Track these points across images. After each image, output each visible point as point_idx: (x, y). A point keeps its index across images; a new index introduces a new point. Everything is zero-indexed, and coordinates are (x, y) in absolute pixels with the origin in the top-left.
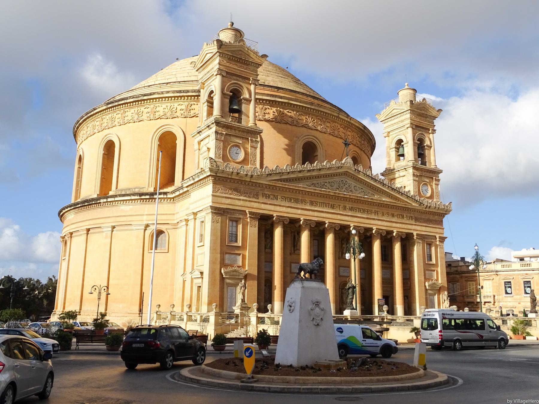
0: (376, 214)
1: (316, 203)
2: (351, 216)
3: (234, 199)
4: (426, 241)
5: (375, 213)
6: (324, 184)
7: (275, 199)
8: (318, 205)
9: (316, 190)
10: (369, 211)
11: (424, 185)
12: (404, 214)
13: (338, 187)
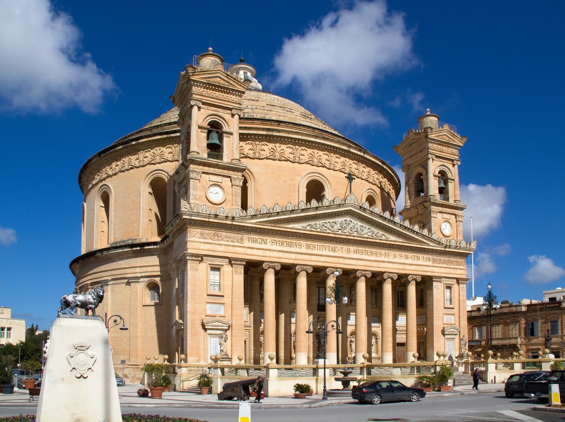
0: (387, 256)
1: (314, 246)
3: (214, 244)
4: (446, 284)
5: (385, 255)
6: (323, 225)
7: (264, 243)
8: (316, 249)
9: (312, 231)
10: (377, 253)
11: (445, 223)
12: (420, 255)
13: (340, 228)
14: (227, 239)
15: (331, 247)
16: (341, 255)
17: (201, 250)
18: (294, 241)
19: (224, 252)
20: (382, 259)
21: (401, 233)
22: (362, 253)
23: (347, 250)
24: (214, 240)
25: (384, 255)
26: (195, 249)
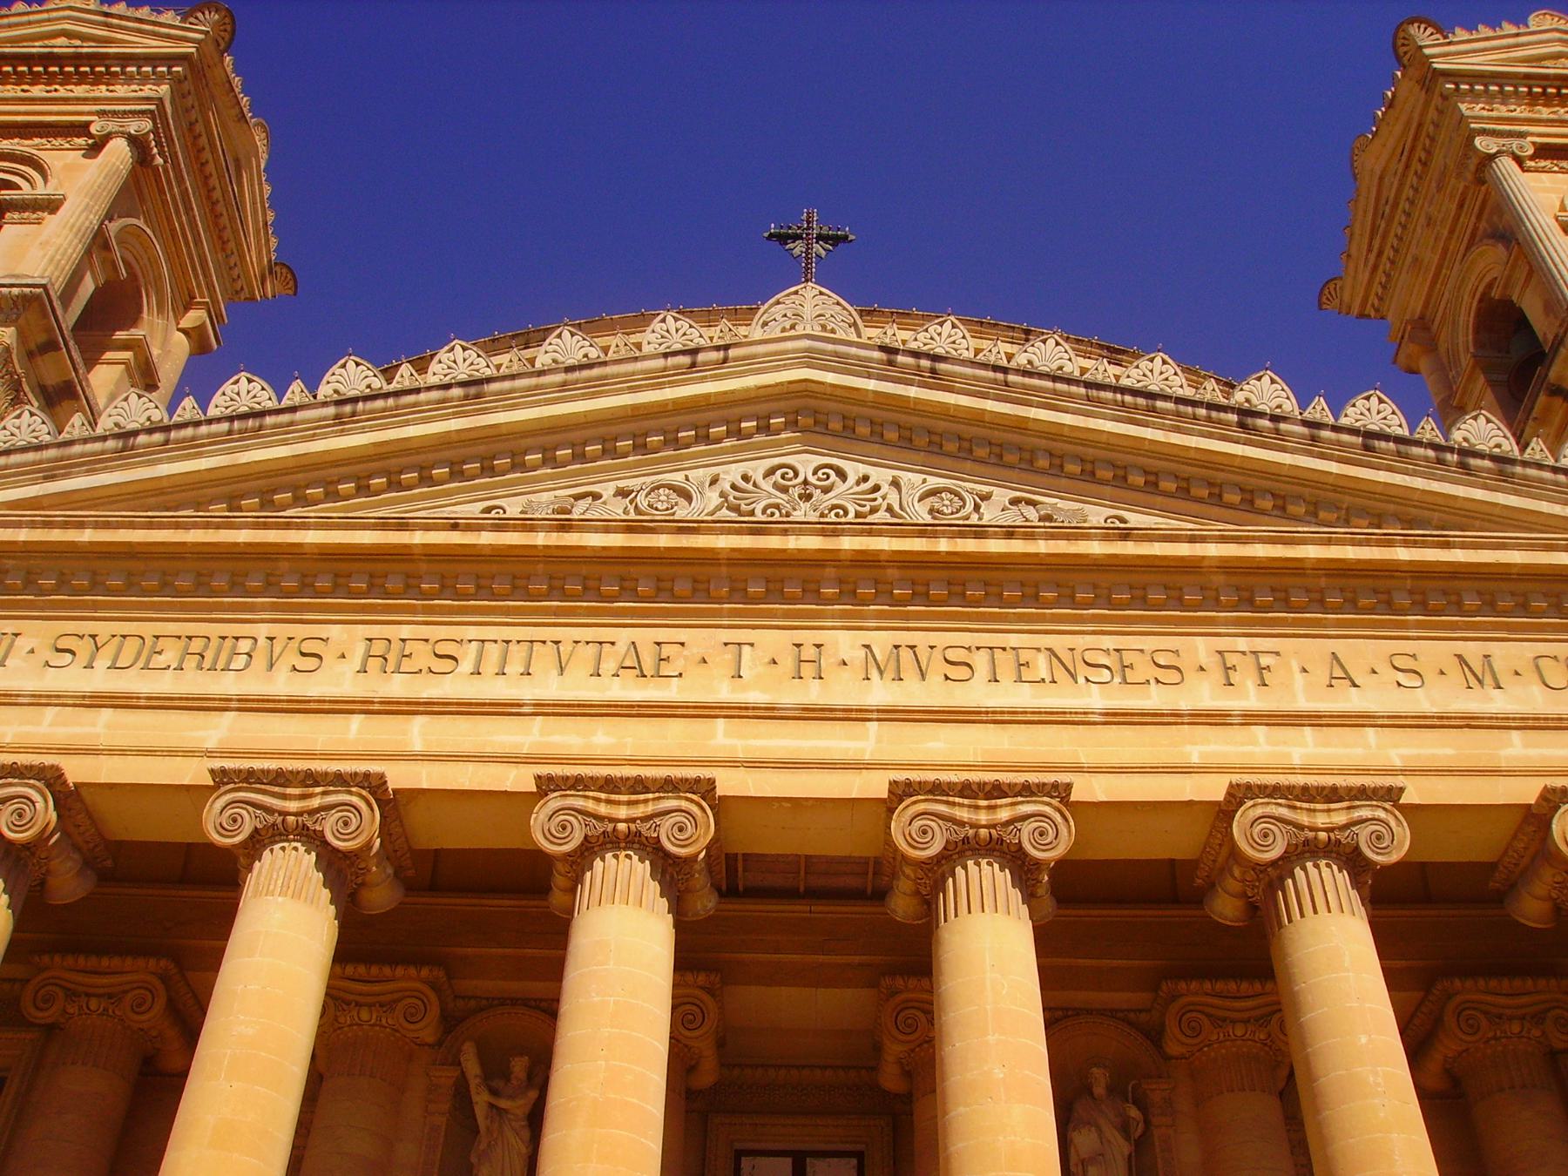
0: (1250, 683)
1: (443, 649)
2: (890, 715)
8: (466, 666)
10: (1128, 658)
15: (622, 647)
16: (725, 693)
18: (262, 630)
20: (1203, 694)
21: (1347, 500)
22: (963, 672)
23: (787, 663)
25: (1217, 675)
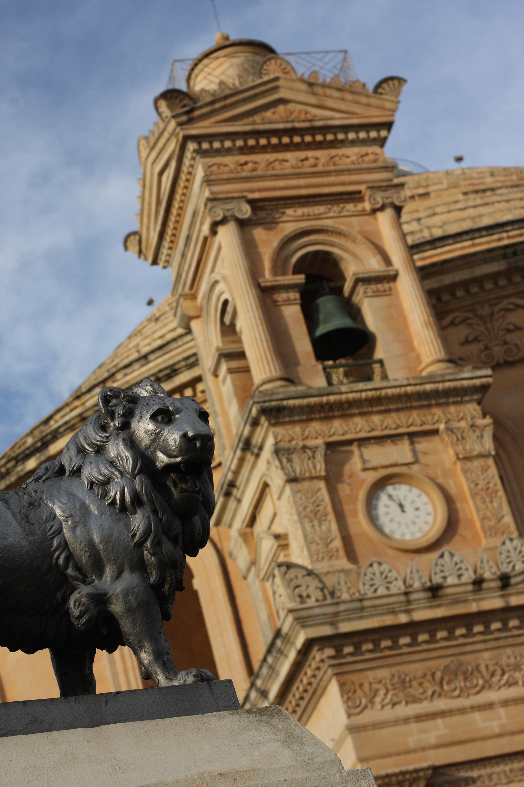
3: (462, 711)
14: (506, 677)
17: (415, 751)
19: (512, 734)
24: (457, 693)
26: (390, 756)
